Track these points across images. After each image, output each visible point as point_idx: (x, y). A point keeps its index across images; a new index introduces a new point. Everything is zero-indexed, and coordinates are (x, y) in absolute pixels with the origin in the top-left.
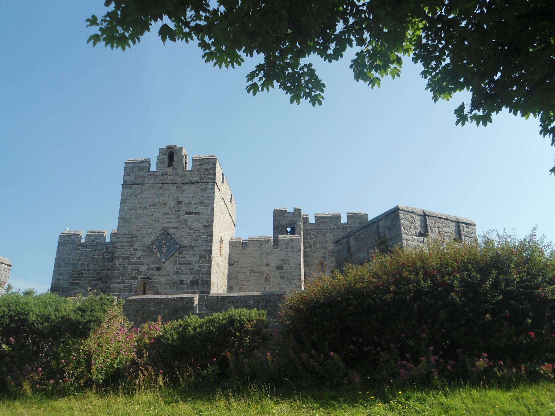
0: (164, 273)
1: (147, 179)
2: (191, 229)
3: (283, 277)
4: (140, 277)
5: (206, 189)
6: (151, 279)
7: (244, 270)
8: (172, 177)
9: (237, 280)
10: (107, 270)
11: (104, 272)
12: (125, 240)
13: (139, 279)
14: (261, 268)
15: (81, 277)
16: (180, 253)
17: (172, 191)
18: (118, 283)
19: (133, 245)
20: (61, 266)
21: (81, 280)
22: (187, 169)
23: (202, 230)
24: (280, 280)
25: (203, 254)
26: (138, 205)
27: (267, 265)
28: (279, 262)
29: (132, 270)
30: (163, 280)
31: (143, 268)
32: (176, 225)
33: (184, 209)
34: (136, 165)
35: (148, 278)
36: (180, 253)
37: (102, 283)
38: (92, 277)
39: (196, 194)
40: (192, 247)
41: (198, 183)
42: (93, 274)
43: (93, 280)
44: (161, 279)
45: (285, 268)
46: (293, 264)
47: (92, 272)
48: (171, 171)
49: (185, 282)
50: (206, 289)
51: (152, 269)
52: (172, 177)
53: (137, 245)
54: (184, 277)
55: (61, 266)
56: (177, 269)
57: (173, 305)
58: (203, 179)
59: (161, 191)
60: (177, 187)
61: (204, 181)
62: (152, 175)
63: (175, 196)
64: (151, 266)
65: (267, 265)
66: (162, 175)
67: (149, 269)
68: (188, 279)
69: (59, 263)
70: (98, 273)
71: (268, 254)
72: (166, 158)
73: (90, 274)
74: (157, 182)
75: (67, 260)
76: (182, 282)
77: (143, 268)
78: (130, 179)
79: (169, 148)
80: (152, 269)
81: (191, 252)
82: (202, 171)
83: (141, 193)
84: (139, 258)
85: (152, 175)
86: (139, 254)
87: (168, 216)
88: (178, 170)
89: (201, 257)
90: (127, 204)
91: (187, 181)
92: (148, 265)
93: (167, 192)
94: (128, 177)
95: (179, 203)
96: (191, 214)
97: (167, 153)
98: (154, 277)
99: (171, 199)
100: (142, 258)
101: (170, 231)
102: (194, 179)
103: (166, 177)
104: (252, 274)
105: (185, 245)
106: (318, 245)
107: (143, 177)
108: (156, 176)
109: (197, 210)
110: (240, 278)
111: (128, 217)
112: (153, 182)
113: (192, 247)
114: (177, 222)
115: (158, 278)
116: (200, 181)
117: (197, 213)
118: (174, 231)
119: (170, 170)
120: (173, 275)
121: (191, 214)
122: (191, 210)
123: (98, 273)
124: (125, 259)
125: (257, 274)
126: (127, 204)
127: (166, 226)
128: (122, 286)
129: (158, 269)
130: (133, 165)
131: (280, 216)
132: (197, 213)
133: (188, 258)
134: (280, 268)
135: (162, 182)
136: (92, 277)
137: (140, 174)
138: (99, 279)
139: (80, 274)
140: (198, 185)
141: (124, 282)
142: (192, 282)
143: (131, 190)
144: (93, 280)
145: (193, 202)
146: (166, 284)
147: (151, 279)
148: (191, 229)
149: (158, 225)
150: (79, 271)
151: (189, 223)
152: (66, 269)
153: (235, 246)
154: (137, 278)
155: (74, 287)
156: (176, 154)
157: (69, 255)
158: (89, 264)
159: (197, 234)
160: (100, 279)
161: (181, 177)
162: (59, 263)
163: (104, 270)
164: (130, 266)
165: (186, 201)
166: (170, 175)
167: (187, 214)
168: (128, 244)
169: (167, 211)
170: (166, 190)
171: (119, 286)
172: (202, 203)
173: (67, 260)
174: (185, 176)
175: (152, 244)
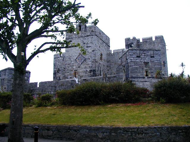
16: (86, 61)
18: (68, 73)
23: (92, 52)
30: (81, 71)
31: (74, 67)
35: (76, 70)
53: (72, 60)
68: (88, 70)
76: (87, 71)
77: (74, 67)
86: (73, 62)
89: (92, 62)
96: (88, 47)
121: (88, 47)
122: (88, 46)
128: (68, 73)
129: (79, 67)
142: (90, 71)
165: (86, 42)
175: (76, 59)
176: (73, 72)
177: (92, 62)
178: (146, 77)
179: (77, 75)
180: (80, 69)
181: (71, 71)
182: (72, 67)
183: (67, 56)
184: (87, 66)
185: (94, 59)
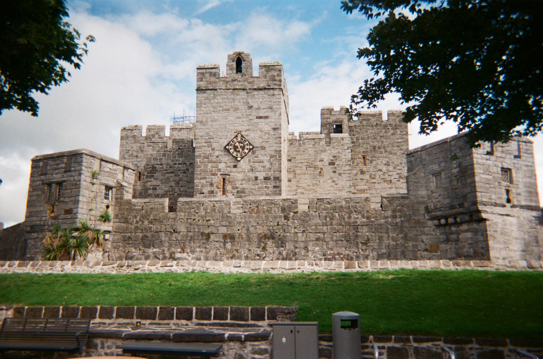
1: (218, 85)
2: (261, 131)
3: (335, 172)
4: (219, 173)
5: (273, 95)
6: (229, 175)
7: (300, 165)
8: (241, 83)
9: (295, 174)
10: (179, 164)
11: (176, 166)
12: (204, 141)
13: (219, 175)
14: (316, 164)
15: (155, 171)
16: (254, 153)
17: (243, 97)
18: (201, 179)
19: (211, 146)
20: (125, 158)
21: (155, 173)
22: (254, 75)
23: (272, 132)
24: (333, 174)
25: (273, 153)
26: (212, 109)
27: (322, 161)
28: (331, 158)
29: (212, 167)
30: (240, 176)
31: (222, 166)
32: (248, 128)
33: (255, 113)
34: (208, 70)
36: (254, 153)
37: (175, 176)
38: (165, 170)
39: (265, 100)
40: (263, 148)
41: (265, 89)
42: (166, 168)
43: (166, 173)
45: (336, 163)
46: (344, 160)
47: (165, 166)
48: (240, 76)
49: (259, 178)
50: (277, 184)
51: (230, 167)
52: (241, 83)
53: (214, 145)
54: (257, 174)
55: (125, 158)
56: (251, 166)
57: (281, 205)
58: (270, 86)
59: (232, 96)
60: (247, 93)
61: (271, 87)
62: (223, 81)
63: (245, 101)
64: (229, 164)
65: (322, 161)
66: (233, 81)
67: (227, 167)
69: (124, 155)
70: (171, 167)
71: (322, 151)
72: (234, 64)
73: (163, 168)
74: (228, 88)
75: (131, 152)
76: (256, 178)
77: (222, 166)
78: (203, 84)
79: (240, 54)
81: (263, 152)
82: (268, 78)
83: (214, 98)
84: (217, 157)
85: (223, 81)
86: (217, 153)
87: (241, 120)
88: (247, 76)
89: (272, 157)
90: (203, 109)
91: (256, 87)
92: (226, 163)
93: (238, 97)
94: (201, 83)
95: (251, 107)
96: (261, 118)
97: (235, 59)
98: (232, 174)
99: (242, 103)
100: (220, 157)
102: (262, 85)
103: (236, 83)
104: (308, 169)
105: (258, 146)
106: (360, 141)
107: (215, 82)
108: (227, 82)
109: (266, 114)
110: (297, 172)
111: (204, 120)
112: (224, 88)
113: (263, 148)
114: (248, 125)
116: (267, 87)
117: (266, 117)
118: (247, 133)
119: (239, 76)
120: (248, 172)
121: (261, 118)
122: (261, 115)
123: (171, 167)
125: (312, 169)
126: (203, 109)
127: (239, 128)
128: (204, 181)
129: (235, 166)
131: (328, 114)
132: (266, 117)
133: (261, 158)
134: (332, 163)
135: (232, 88)
136: (165, 170)
137: (213, 79)
138: (172, 173)
139: (154, 168)
140: (266, 91)
141: (206, 178)
142: (265, 179)
143: (205, 95)
144: (166, 173)
145: (262, 107)
146: (242, 180)
147: (229, 175)
148: (261, 131)
149: (232, 128)
150: (153, 165)
151: (259, 127)
152: (131, 160)
153: (291, 144)
154: (217, 175)
155: (149, 179)
156: (244, 61)
157: (132, 148)
158: (161, 159)
160: (173, 173)
161: (249, 83)
162: (124, 155)
163: (175, 164)
164: (210, 164)
165: (255, 106)
166: (239, 81)
167: (257, 118)
168: (206, 145)
169: (240, 115)
170: (237, 95)
171: (202, 181)
172: (271, 108)
173: (131, 152)
174: (253, 82)
175: (228, 145)
176: (217, 179)
177: (272, 157)
178: (508, 205)
179: (229, 187)
180: (239, 172)
181: (213, 175)
182: (214, 165)
183: (201, 134)
184: (257, 165)
185: (276, 151)
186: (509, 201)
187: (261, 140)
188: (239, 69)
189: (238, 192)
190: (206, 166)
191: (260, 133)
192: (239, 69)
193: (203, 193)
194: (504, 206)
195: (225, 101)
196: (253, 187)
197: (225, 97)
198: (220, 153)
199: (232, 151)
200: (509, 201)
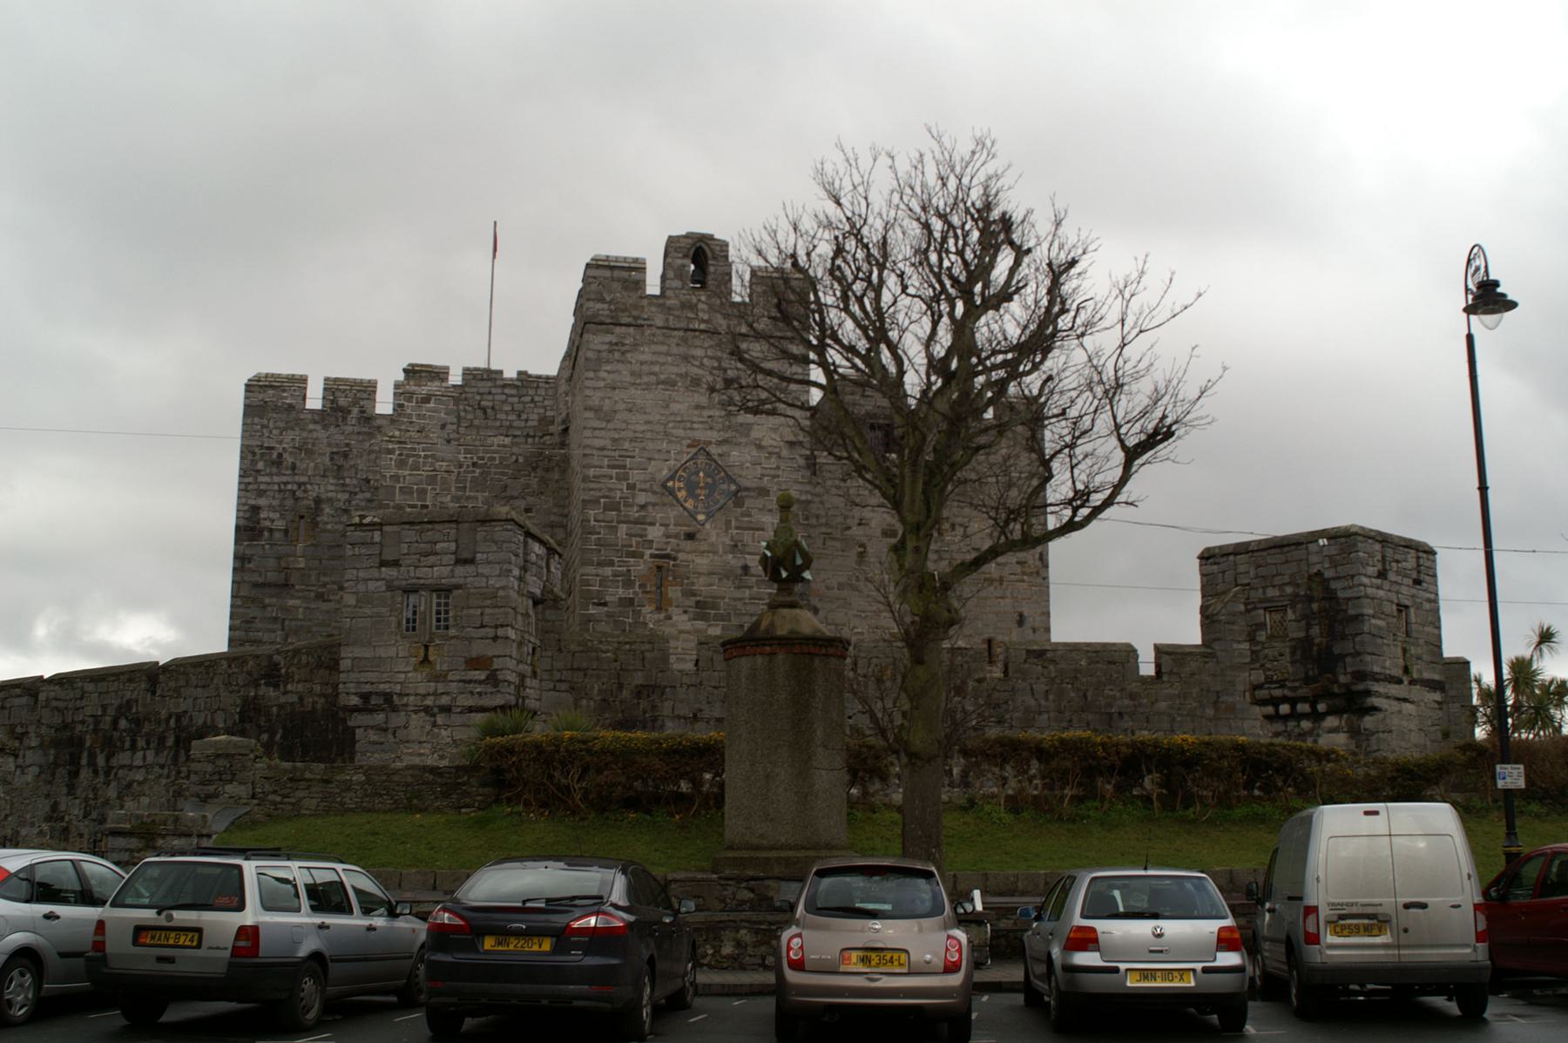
0: (704, 547)
2: (760, 447)
4: (648, 552)
13: (647, 557)
16: (739, 503)
23: (785, 453)
26: (629, 379)
31: (654, 533)
34: (616, 273)
35: (667, 556)
40: (763, 492)
44: (699, 560)
51: (676, 536)
53: (636, 476)
59: (682, 350)
64: (673, 529)
74: (671, 324)
76: (746, 568)
77: (654, 533)
80: (676, 536)
81: (759, 503)
84: (643, 507)
86: (642, 498)
92: (666, 526)
98: (681, 556)
100: (650, 508)
101: (713, 450)
113: (763, 492)
115: (690, 557)
124: (607, 508)
127: (701, 435)
128: (608, 571)
129: (690, 536)
130: (608, 273)
135: (683, 325)
141: (611, 563)
146: (711, 574)
147: (675, 559)
148: (760, 447)
149: (680, 432)
154: (642, 556)
159: (773, 462)
175: (672, 478)
179: (674, 592)
181: (633, 555)
182: (637, 529)
184: (747, 536)
186: (1406, 670)
187: (759, 470)
188: (701, 277)
189: (698, 603)
190: (614, 530)
191: (755, 453)
192: (701, 277)
193: (605, 604)
194: (1400, 682)
195: (662, 359)
196: (738, 594)
197: (664, 348)
198: (652, 498)
199: (682, 494)
200: (1406, 670)
